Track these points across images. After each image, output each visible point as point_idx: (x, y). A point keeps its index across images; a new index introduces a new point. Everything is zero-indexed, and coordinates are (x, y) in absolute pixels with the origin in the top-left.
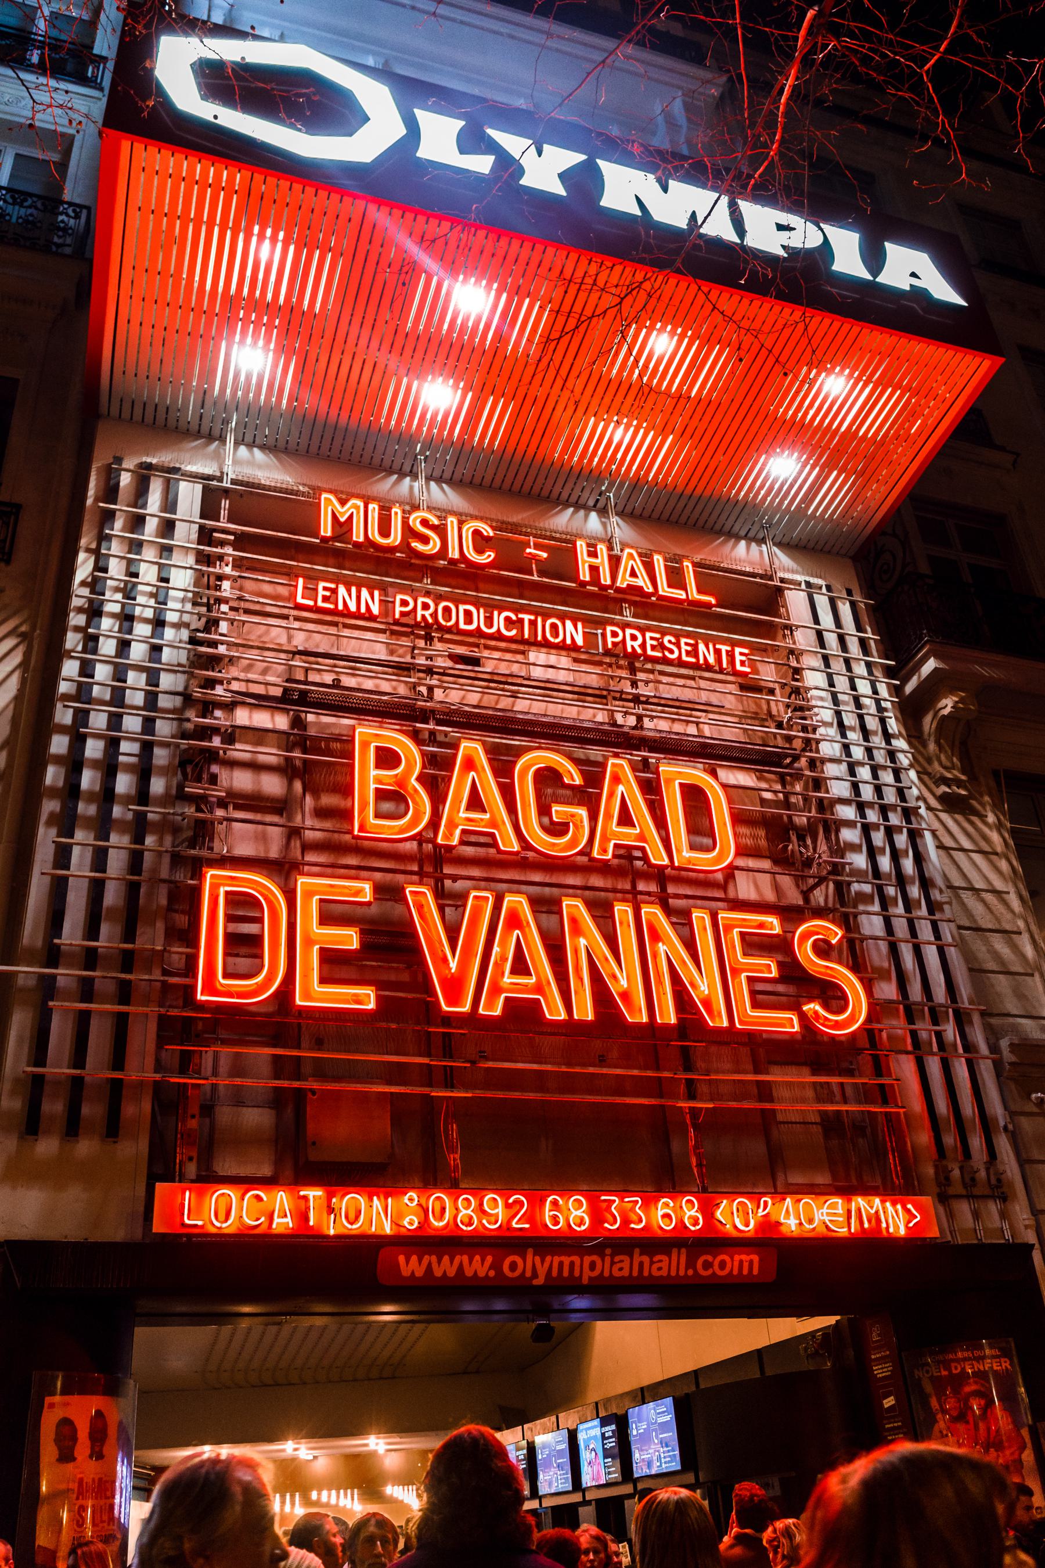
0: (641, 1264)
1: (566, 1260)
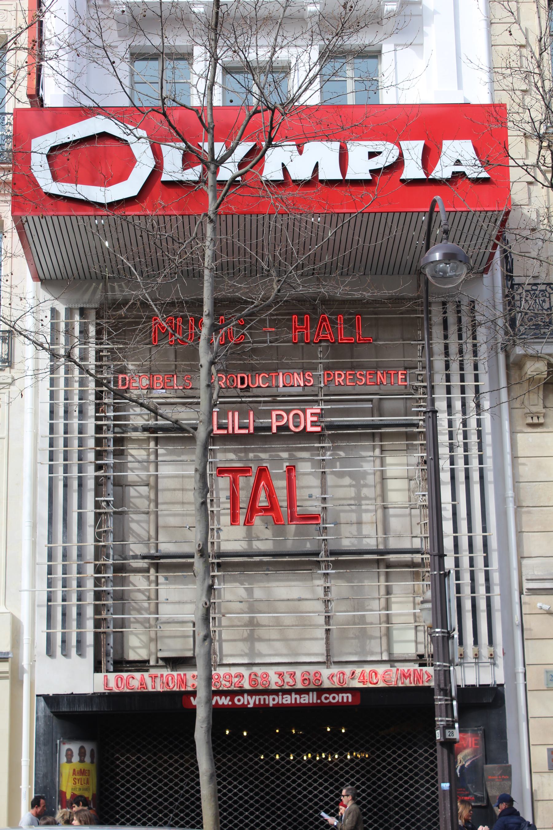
0: (296, 699)
1: (262, 698)
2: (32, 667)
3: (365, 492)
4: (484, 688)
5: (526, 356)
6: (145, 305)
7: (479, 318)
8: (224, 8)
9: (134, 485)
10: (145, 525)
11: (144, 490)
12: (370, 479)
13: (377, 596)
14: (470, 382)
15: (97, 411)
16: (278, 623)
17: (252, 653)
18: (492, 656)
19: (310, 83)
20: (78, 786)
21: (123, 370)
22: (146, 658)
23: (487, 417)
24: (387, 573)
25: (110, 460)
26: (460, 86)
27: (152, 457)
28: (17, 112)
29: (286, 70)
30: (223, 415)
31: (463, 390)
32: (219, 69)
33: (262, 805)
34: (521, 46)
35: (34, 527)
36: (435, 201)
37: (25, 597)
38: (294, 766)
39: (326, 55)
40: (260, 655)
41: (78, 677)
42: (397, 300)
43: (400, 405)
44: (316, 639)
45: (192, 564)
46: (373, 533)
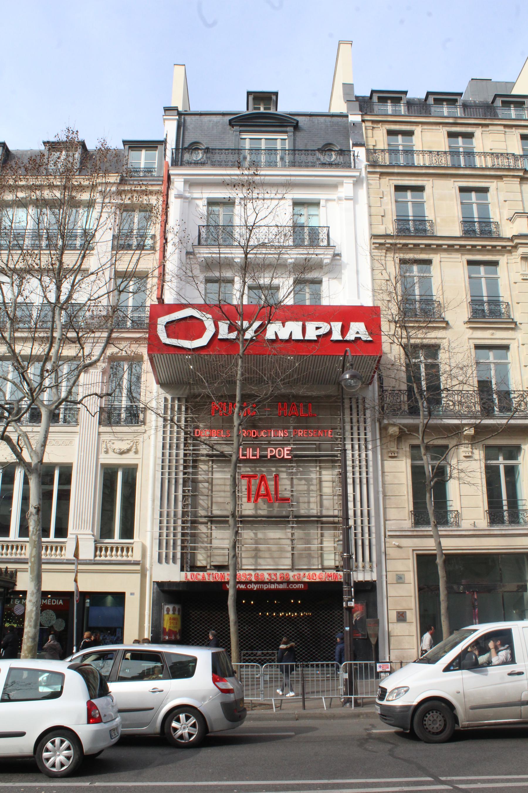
2: (151, 568)
3: (312, 487)
4: (367, 582)
5: (389, 424)
6: (209, 397)
7: (367, 406)
8: (249, 260)
9: (201, 482)
10: (206, 502)
11: (206, 485)
12: (315, 482)
13: (316, 537)
14: (362, 436)
15: (185, 446)
16: (269, 550)
17: (256, 564)
18: (371, 567)
19: (289, 294)
20: (172, 625)
21: (197, 427)
22: (205, 565)
23: (370, 453)
24: (322, 527)
25: (190, 470)
26: (359, 297)
27: (210, 469)
28: (152, 306)
29: (277, 288)
30: (244, 449)
31: (359, 440)
32: (246, 287)
33: (260, 637)
34: (387, 280)
35: (153, 501)
36: (346, 351)
37: (149, 535)
38: (275, 618)
39: (297, 282)
40: (260, 565)
41: (173, 573)
42: (328, 397)
43: (329, 446)
44: (287, 558)
45: (228, 521)
46: (315, 508)
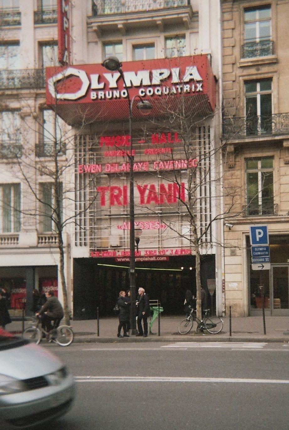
1: (139, 258)
